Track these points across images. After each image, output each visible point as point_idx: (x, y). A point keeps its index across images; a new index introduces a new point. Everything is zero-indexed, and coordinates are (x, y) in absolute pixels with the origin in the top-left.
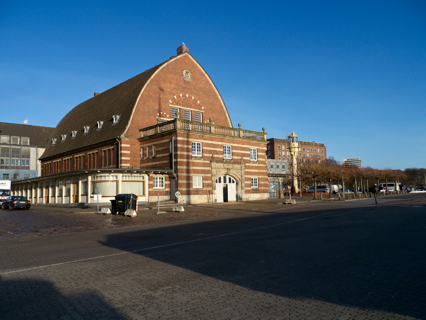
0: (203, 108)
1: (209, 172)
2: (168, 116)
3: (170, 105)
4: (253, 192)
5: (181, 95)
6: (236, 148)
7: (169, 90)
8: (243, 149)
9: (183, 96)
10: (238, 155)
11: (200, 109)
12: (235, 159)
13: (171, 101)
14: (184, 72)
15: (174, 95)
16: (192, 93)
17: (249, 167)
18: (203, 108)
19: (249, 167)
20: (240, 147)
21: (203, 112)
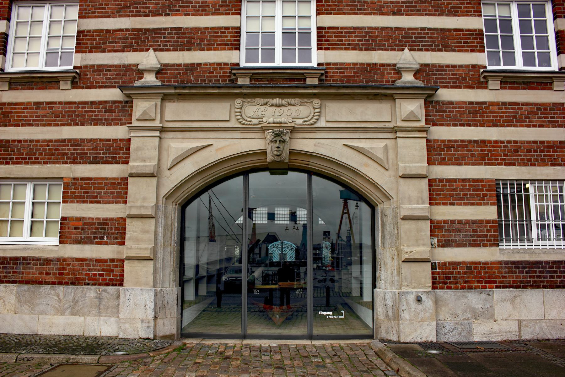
1: (118, 151)
4: (517, 276)
12: (341, 67)
17: (478, 114)
19: (478, 114)
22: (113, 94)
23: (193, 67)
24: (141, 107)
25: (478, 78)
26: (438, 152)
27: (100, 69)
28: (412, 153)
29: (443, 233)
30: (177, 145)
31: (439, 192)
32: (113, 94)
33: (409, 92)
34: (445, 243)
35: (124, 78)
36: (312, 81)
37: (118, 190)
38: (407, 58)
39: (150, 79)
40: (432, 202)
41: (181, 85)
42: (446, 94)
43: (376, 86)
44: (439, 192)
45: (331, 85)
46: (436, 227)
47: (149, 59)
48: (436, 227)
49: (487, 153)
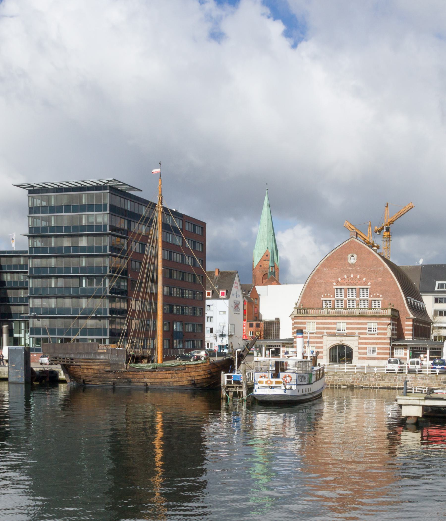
0: (369, 284)
1: (321, 343)
2: (332, 296)
3: (334, 287)
5: (345, 277)
6: (351, 324)
7: (333, 274)
8: (358, 324)
9: (347, 277)
10: (352, 329)
11: (366, 285)
12: (349, 333)
13: (335, 284)
14: (349, 256)
15: (338, 278)
16: (357, 272)
17: (365, 339)
18: (369, 284)
19: (365, 339)
20: (355, 323)
21: (369, 287)
22: (321, 335)
23: (330, 332)
24: (324, 337)
25: (365, 334)
26: (360, 343)
27: (319, 332)
28: (357, 343)
29: (360, 353)
30: (329, 342)
31: (359, 348)
32: (321, 335)
33: (357, 336)
34: (360, 354)
35: (322, 333)
36: (345, 335)
37: (322, 347)
38: (357, 331)
39: (325, 334)
40: (359, 349)
41: (329, 334)
42: (361, 336)
43: (352, 335)
44: (359, 348)
45: (348, 335)
46: (359, 353)
47: (325, 331)
48: (359, 353)
49: (366, 344)
